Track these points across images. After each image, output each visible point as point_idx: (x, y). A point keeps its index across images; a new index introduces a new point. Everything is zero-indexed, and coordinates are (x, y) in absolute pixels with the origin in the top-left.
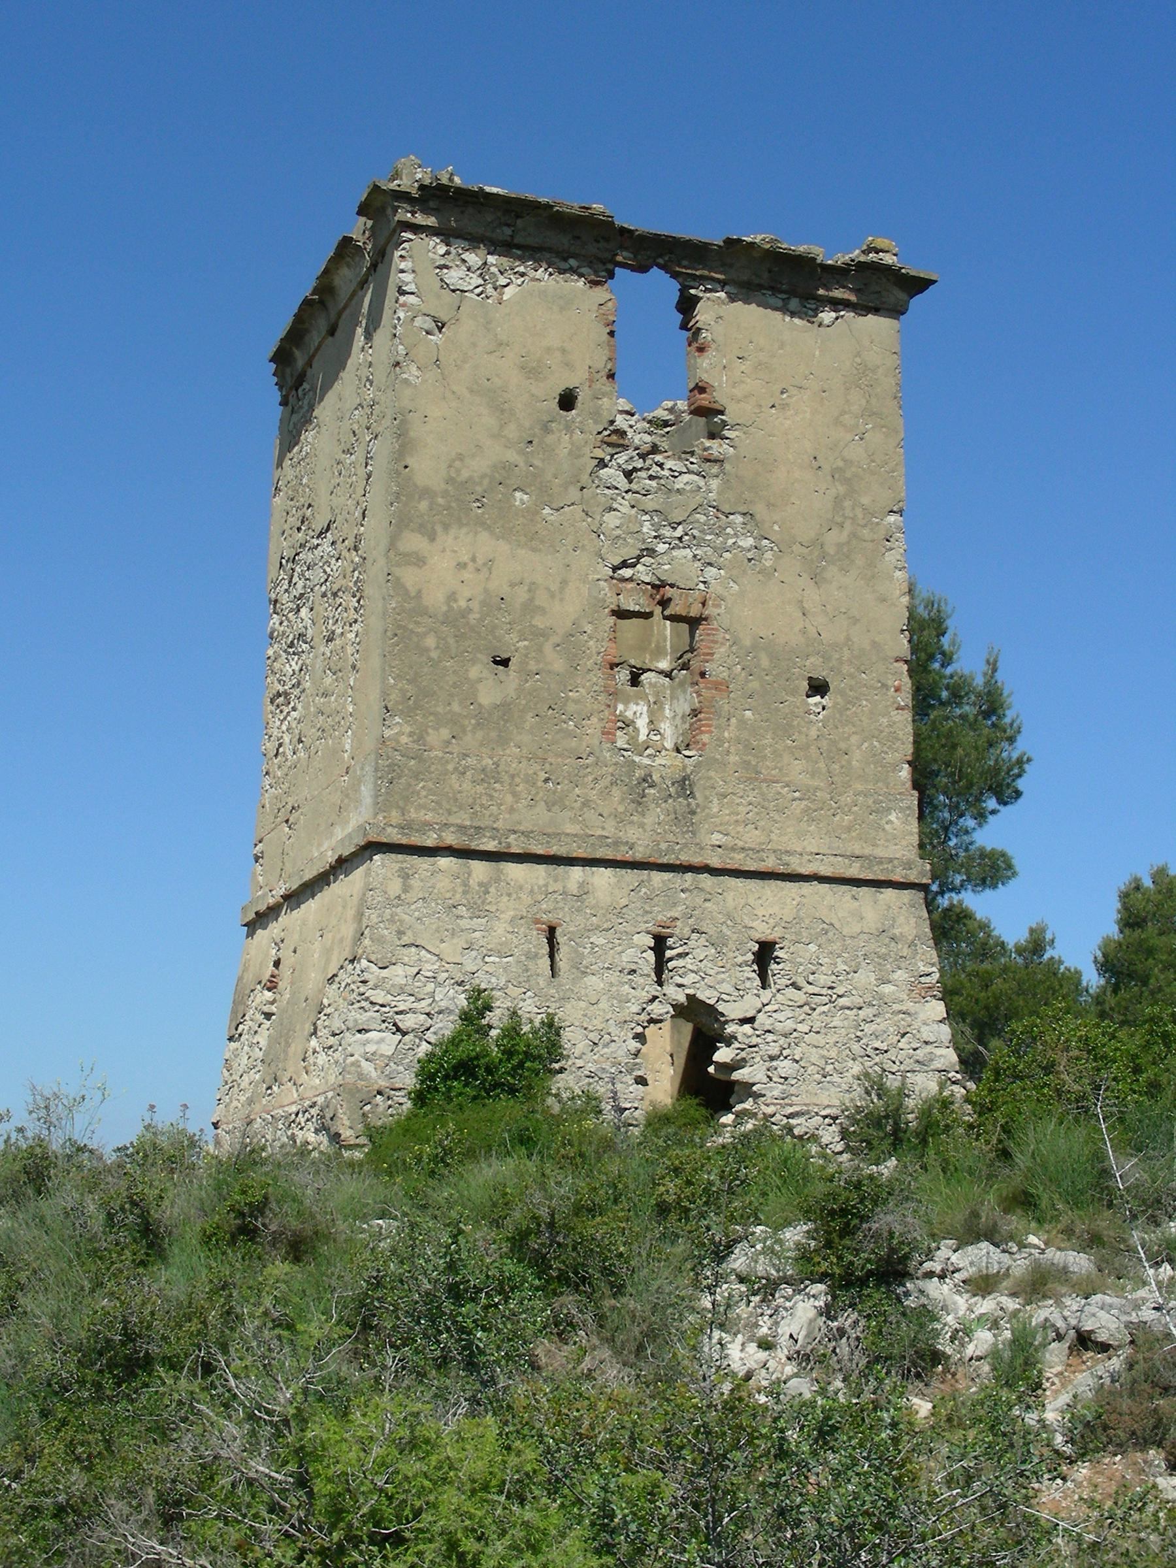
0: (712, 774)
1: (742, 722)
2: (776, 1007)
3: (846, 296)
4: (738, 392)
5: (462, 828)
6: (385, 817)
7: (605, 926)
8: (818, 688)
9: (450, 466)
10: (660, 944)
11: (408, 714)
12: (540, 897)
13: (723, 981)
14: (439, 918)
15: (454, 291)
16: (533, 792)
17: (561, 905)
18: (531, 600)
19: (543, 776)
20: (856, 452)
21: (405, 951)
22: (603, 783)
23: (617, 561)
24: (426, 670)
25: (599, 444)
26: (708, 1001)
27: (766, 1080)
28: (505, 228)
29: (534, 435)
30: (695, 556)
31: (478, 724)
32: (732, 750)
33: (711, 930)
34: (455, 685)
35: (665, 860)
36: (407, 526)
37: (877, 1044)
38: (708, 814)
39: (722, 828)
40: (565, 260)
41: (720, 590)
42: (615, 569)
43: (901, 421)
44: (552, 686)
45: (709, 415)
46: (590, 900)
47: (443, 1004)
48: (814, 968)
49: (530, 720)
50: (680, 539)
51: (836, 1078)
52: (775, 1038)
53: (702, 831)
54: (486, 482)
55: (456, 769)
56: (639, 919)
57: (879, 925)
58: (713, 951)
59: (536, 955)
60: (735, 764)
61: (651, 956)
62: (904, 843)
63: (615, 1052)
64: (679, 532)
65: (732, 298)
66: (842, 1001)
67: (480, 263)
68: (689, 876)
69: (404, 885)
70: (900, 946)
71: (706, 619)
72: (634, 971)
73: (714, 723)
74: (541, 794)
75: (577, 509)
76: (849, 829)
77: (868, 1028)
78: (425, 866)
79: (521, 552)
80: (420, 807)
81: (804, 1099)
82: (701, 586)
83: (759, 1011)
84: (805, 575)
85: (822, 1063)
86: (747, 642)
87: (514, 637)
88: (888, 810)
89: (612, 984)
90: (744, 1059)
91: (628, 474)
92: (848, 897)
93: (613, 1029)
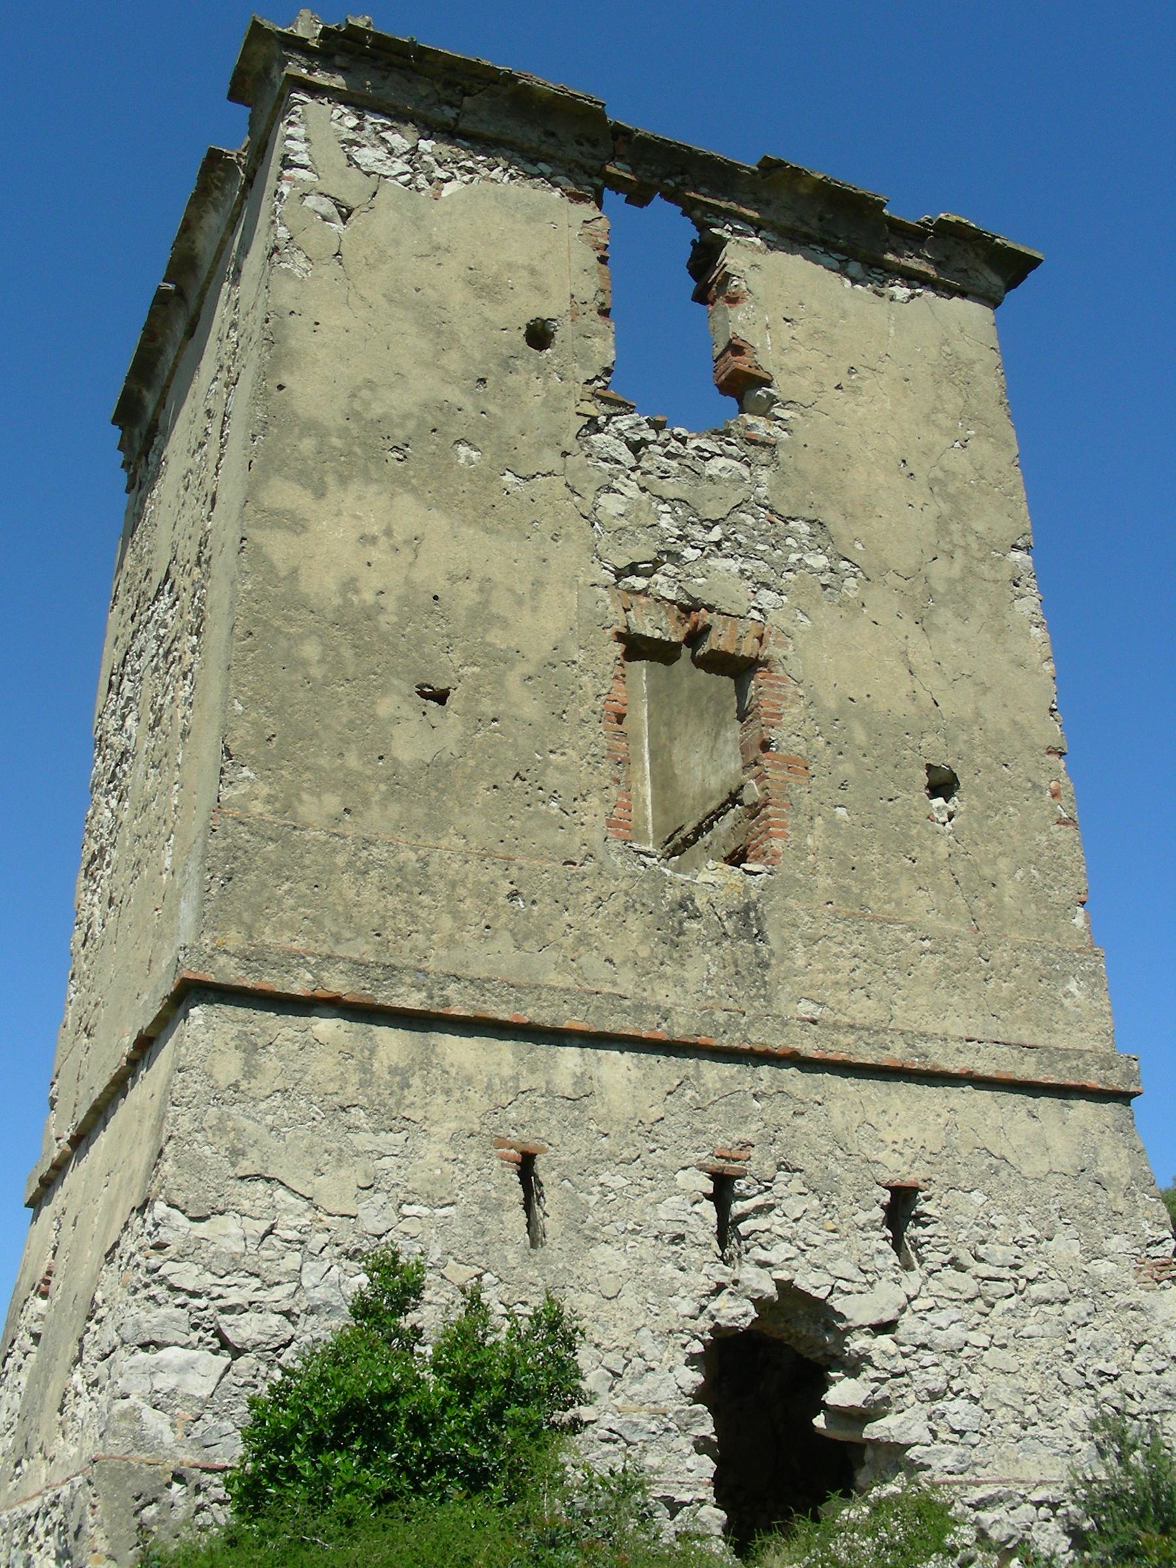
0: (791, 902)
1: (833, 825)
2: (930, 1302)
3: (923, 269)
4: (790, 361)
5: (359, 966)
6: (214, 939)
7: (626, 1154)
8: (942, 784)
9: (353, 395)
10: (723, 1189)
11: (266, 768)
12: (505, 1099)
13: (837, 1256)
14: (313, 1129)
15: (368, 174)
16: (490, 914)
17: (543, 1113)
18: (485, 604)
19: (507, 888)
20: (958, 461)
21: (246, 1188)
22: (613, 906)
23: (623, 562)
24: (301, 695)
25: (589, 397)
26: (815, 1293)
27: (928, 1437)
28: (446, 108)
29: (489, 372)
30: (742, 571)
31: (393, 792)
32: (821, 866)
33: (810, 1166)
34: (351, 725)
35: (724, 1041)
36: (278, 471)
37: (1101, 1365)
38: (789, 970)
39: (813, 993)
40: (534, 162)
41: (784, 623)
42: (619, 574)
43: (1013, 433)
44: (521, 741)
45: (743, 386)
46: (597, 1108)
47: (318, 1295)
48: (984, 1233)
49: (483, 794)
50: (718, 544)
51: (1042, 1429)
52: (934, 1358)
53: (781, 995)
54: (411, 424)
55: (350, 864)
56: (685, 1143)
57: (1075, 1160)
58: (816, 1202)
59: (500, 1205)
60: (826, 890)
61: (708, 1210)
62: (1094, 1028)
63: (654, 1391)
64: (716, 534)
65: (772, 247)
66: (1037, 1290)
67: (408, 147)
68: (765, 1071)
69: (247, 1062)
70: (1111, 1195)
71: (765, 664)
72: (681, 1238)
73: (790, 821)
74: (503, 919)
75: (559, 482)
76: (1011, 1004)
77: (1084, 1337)
78: (289, 1032)
79: (468, 532)
80: (283, 925)
81: (999, 1470)
82: (755, 614)
83: (903, 1310)
84: (906, 617)
85: (1017, 1402)
86: (831, 704)
87: (456, 657)
88: (1065, 975)
89: (642, 1261)
90: (886, 1400)
91: (636, 447)
92: (1022, 1114)
93: (651, 1349)
